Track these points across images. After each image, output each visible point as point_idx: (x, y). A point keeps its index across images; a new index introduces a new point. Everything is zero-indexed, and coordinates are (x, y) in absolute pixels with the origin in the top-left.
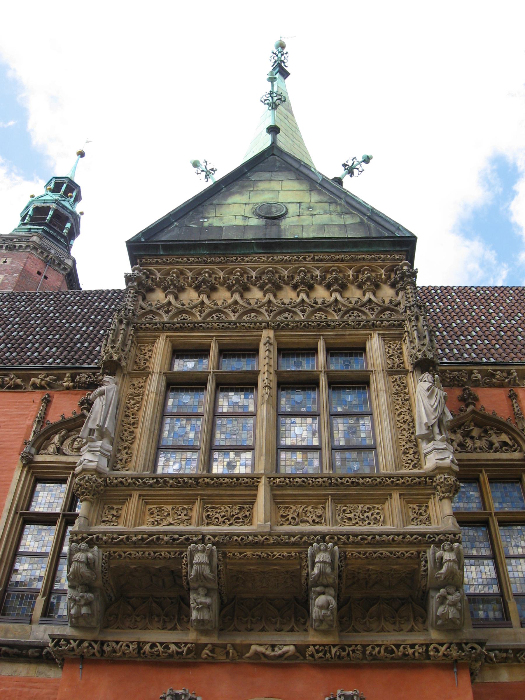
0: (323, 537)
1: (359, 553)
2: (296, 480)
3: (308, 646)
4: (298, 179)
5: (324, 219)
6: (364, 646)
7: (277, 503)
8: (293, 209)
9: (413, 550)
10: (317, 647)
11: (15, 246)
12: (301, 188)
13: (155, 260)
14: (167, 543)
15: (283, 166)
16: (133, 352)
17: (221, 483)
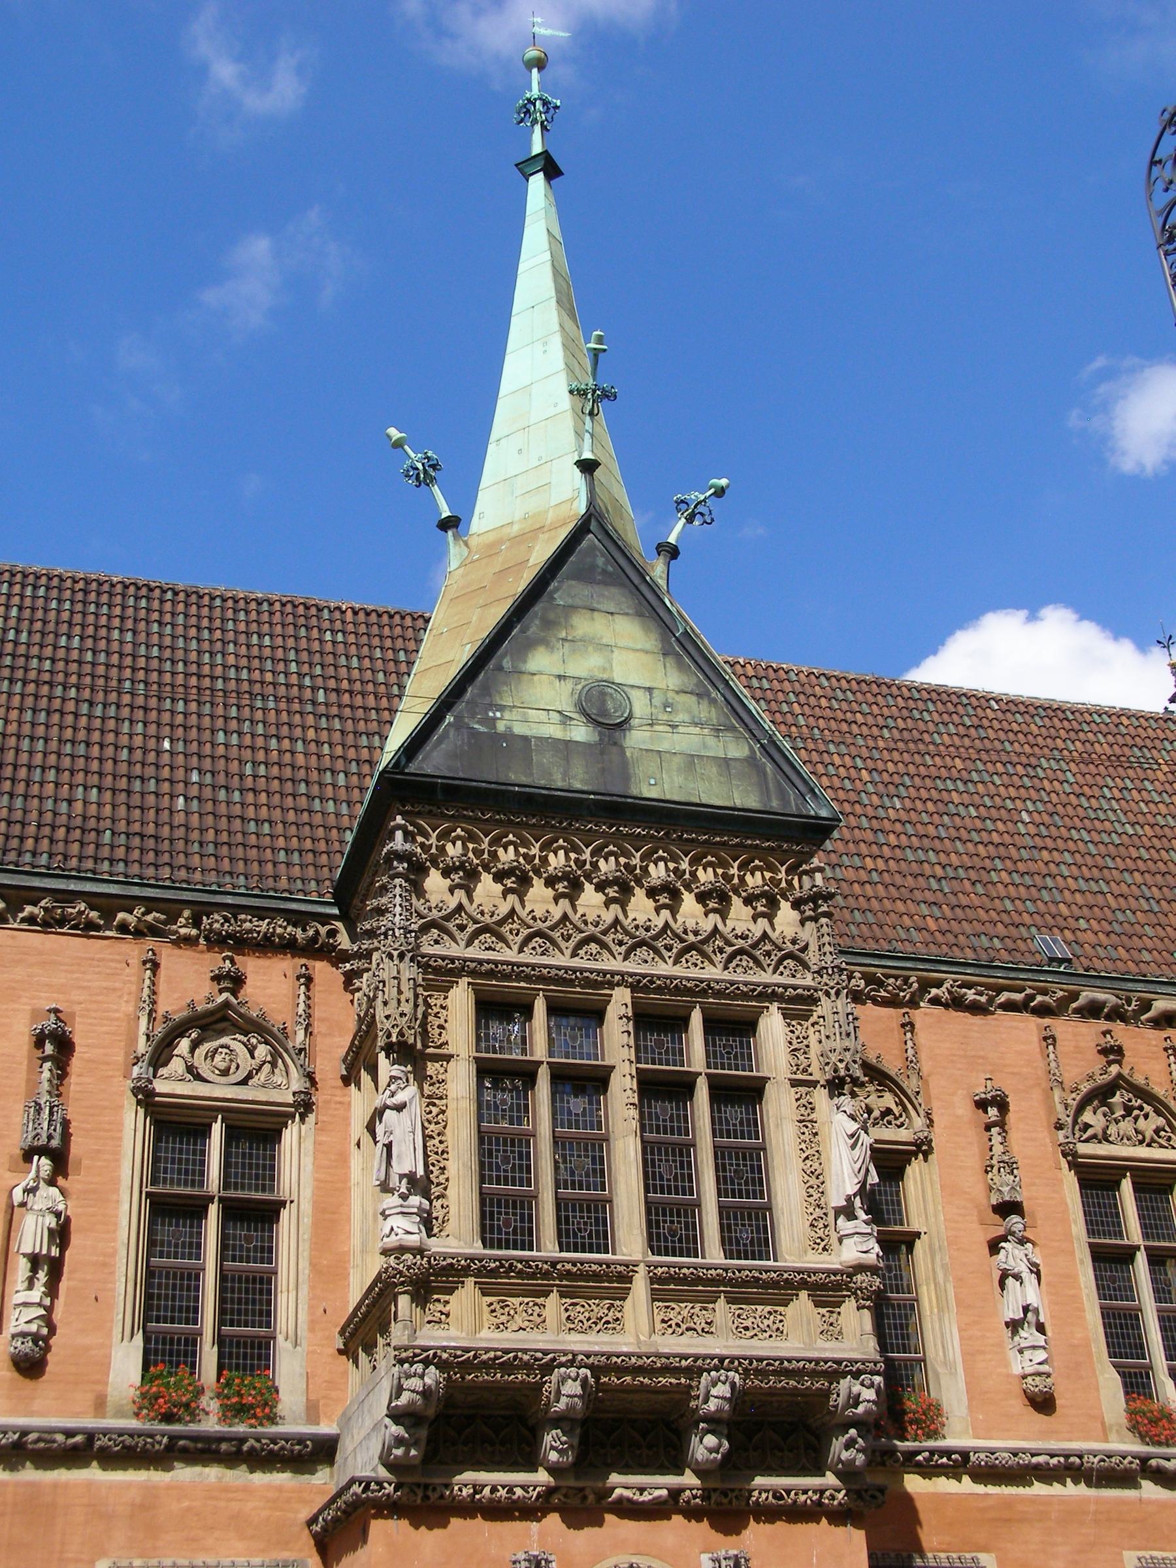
4: (639, 614)
5: (689, 739)
8: (640, 706)
10: (694, 1492)
13: (427, 808)
15: (610, 569)
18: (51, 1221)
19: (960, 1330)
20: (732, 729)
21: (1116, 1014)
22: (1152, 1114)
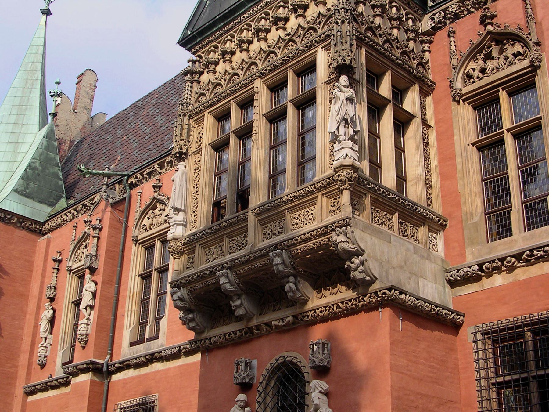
0: (276, 246)
1: (297, 250)
2: (265, 207)
3: (298, 315)
7: (262, 225)
14: (209, 275)
17: (231, 223)
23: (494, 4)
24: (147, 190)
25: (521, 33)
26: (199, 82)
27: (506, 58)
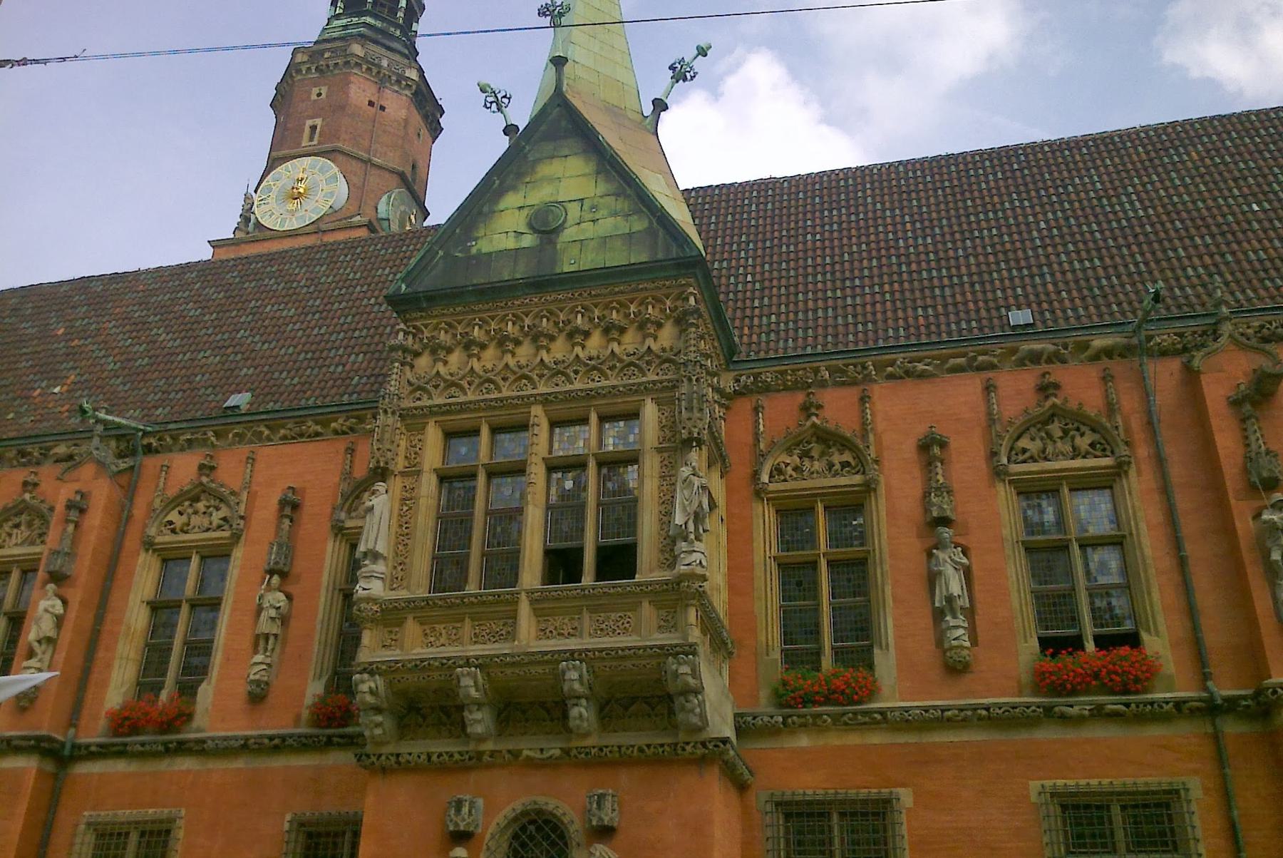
4: (585, 151)
5: (608, 225)
6: (619, 747)
8: (574, 211)
9: (654, 662)
11: (328, 66)
12: (587, 171)
16: (403, 443)
18: (273, 613)
19: (895, 619)
20: (638, 212)
21: (1055, 358)
22: (1088, 432)
23: (822, 390)
24: (183, 468)
25: (858, 441)
26: (412, 367)
27: (831, 465)
